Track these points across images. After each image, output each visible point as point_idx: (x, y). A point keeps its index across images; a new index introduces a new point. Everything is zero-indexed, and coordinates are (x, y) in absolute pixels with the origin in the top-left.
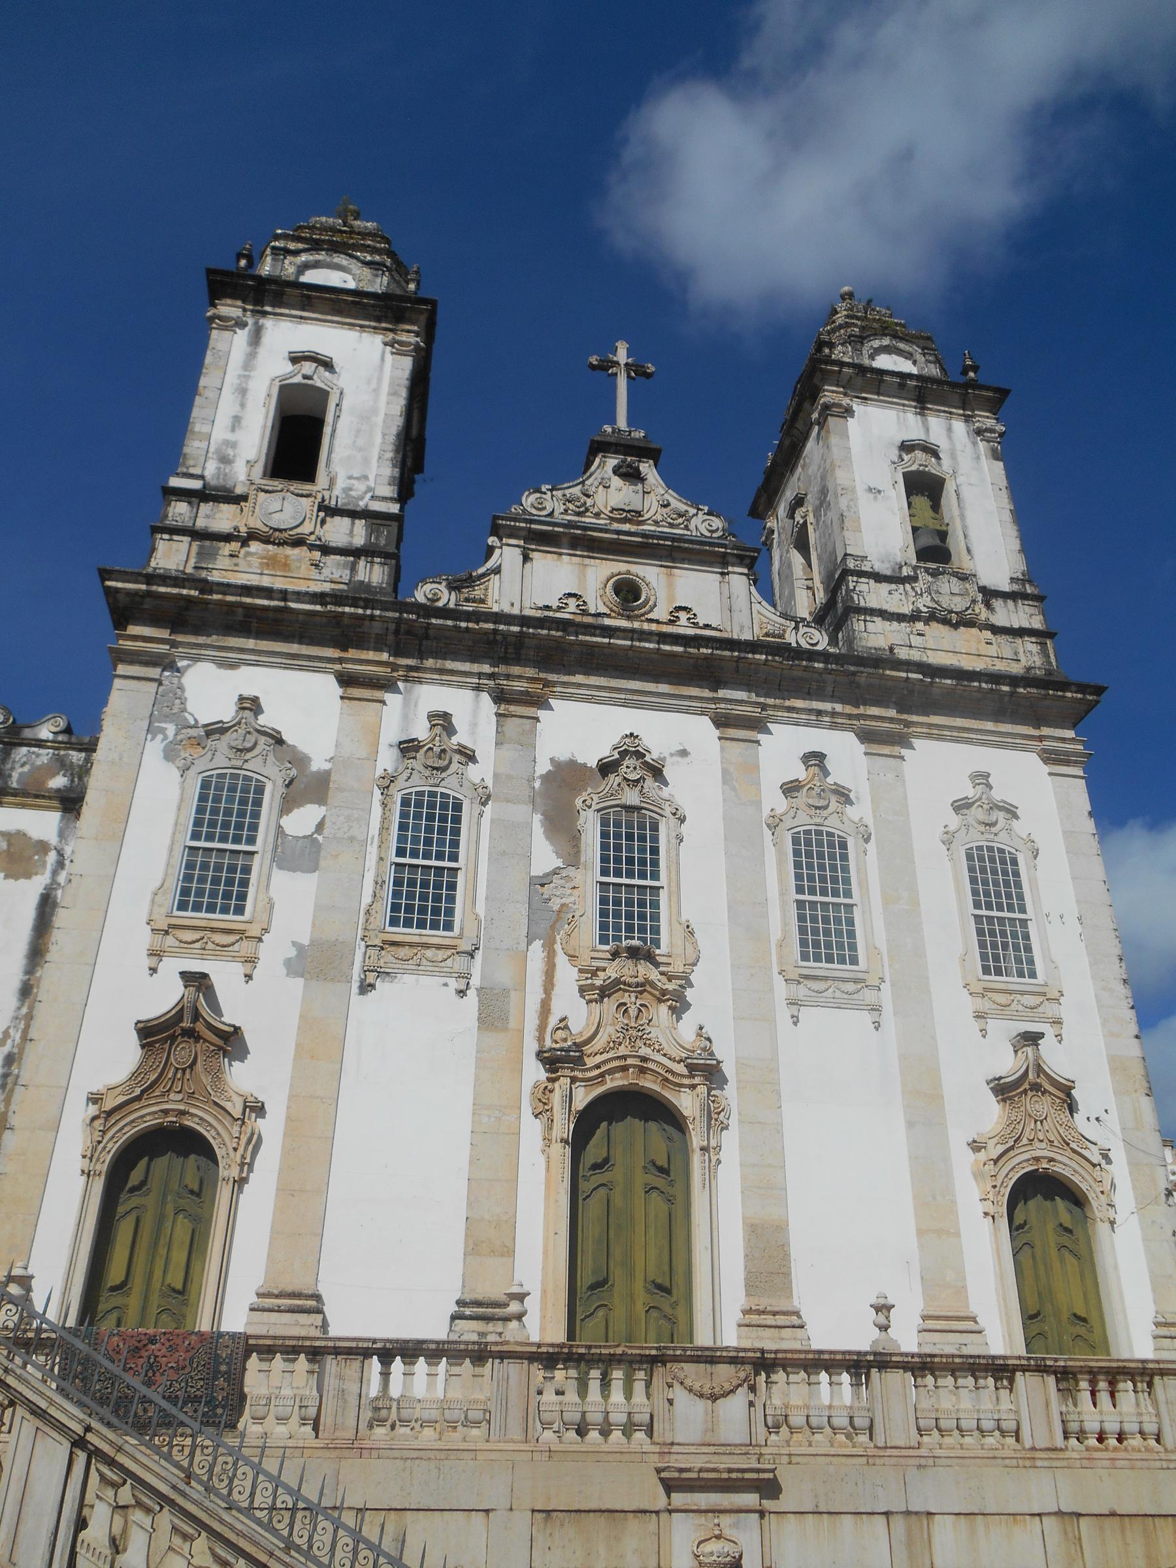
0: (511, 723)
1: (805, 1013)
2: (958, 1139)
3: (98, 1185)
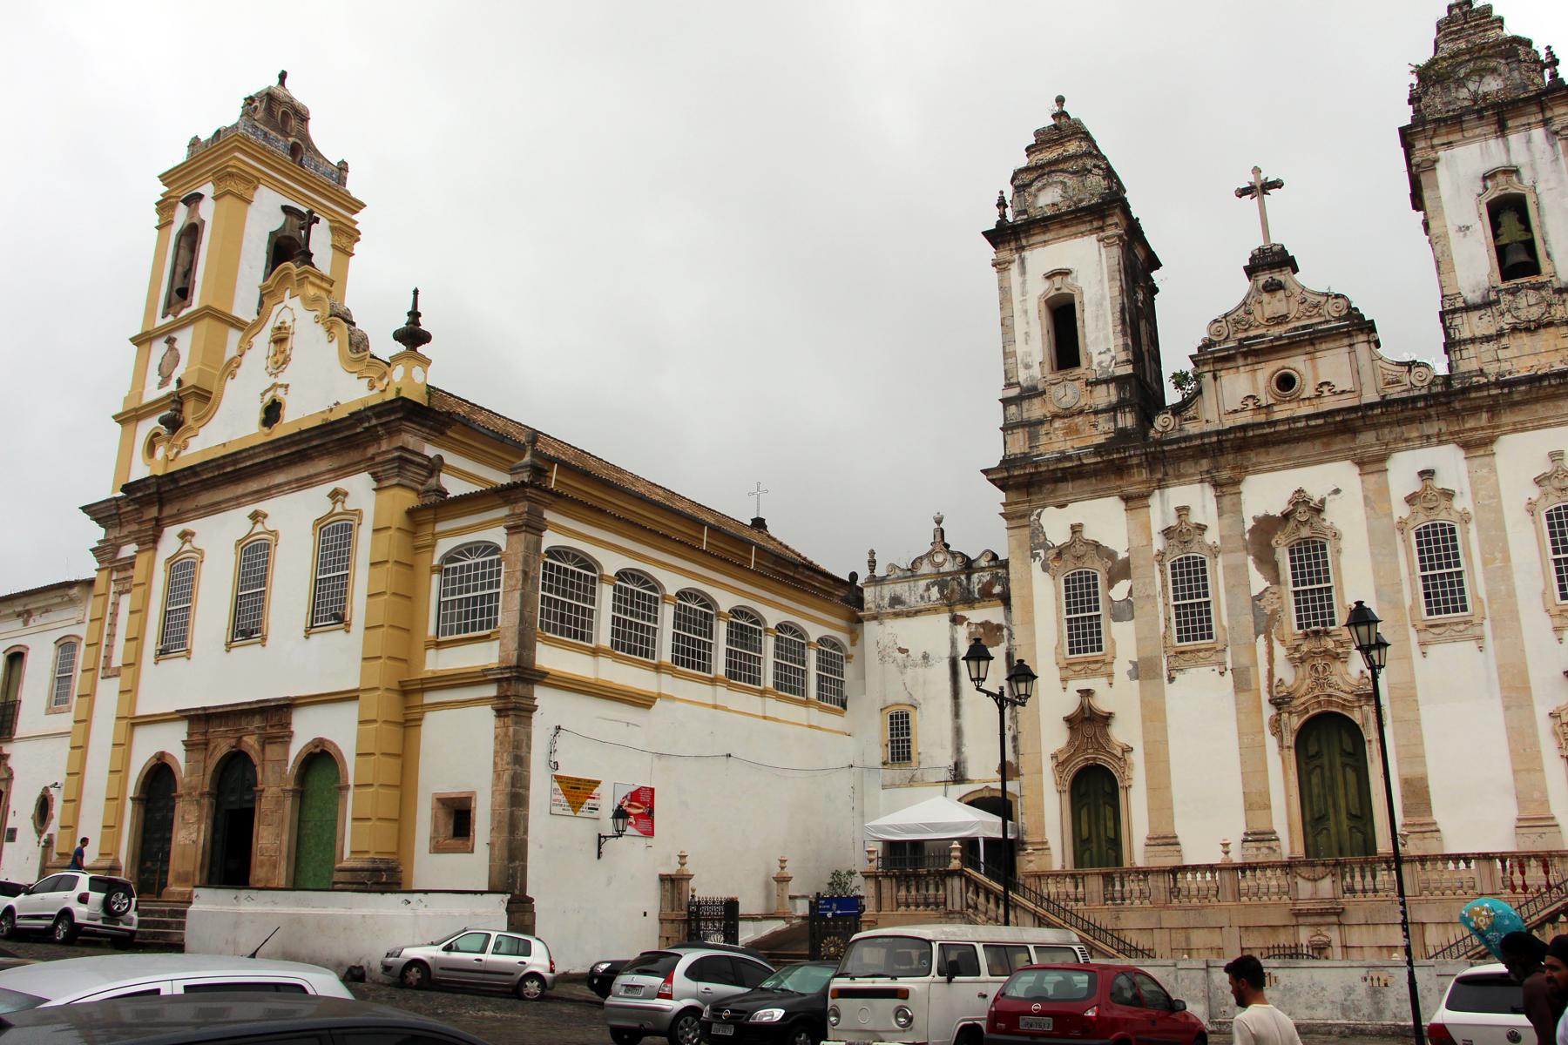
0: (1227, 501)
1: (1431, 650)
2: (1541, 711)
3: (1066, 797)
